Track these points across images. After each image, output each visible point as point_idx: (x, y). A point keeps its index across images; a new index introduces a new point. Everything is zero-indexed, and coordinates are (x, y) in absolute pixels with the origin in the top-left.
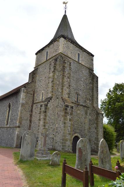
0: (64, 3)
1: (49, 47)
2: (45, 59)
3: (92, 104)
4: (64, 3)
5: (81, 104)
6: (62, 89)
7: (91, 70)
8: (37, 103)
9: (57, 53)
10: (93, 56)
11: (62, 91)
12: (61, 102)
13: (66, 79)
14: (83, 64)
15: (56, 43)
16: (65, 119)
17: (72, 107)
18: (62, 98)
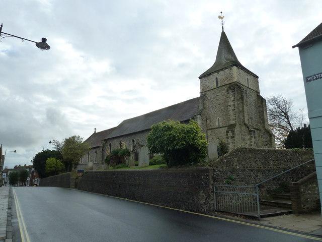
0: (220, 17)
1: (218, 73)
2: (215, 84)
3: (264, 127)
4: (220, 17)
5: (255, 127)
6: (244, 116)
7: (258, 93)
8: (212, 129)
9: (231, 81)
10: (258, 77)
11: (244, 118)
12: (244, 128)
13: (245, 107)
14: (252, 88)
15: (227, 71)
16: (251, 142)
17: (254, 132)
18: (245, 124)
